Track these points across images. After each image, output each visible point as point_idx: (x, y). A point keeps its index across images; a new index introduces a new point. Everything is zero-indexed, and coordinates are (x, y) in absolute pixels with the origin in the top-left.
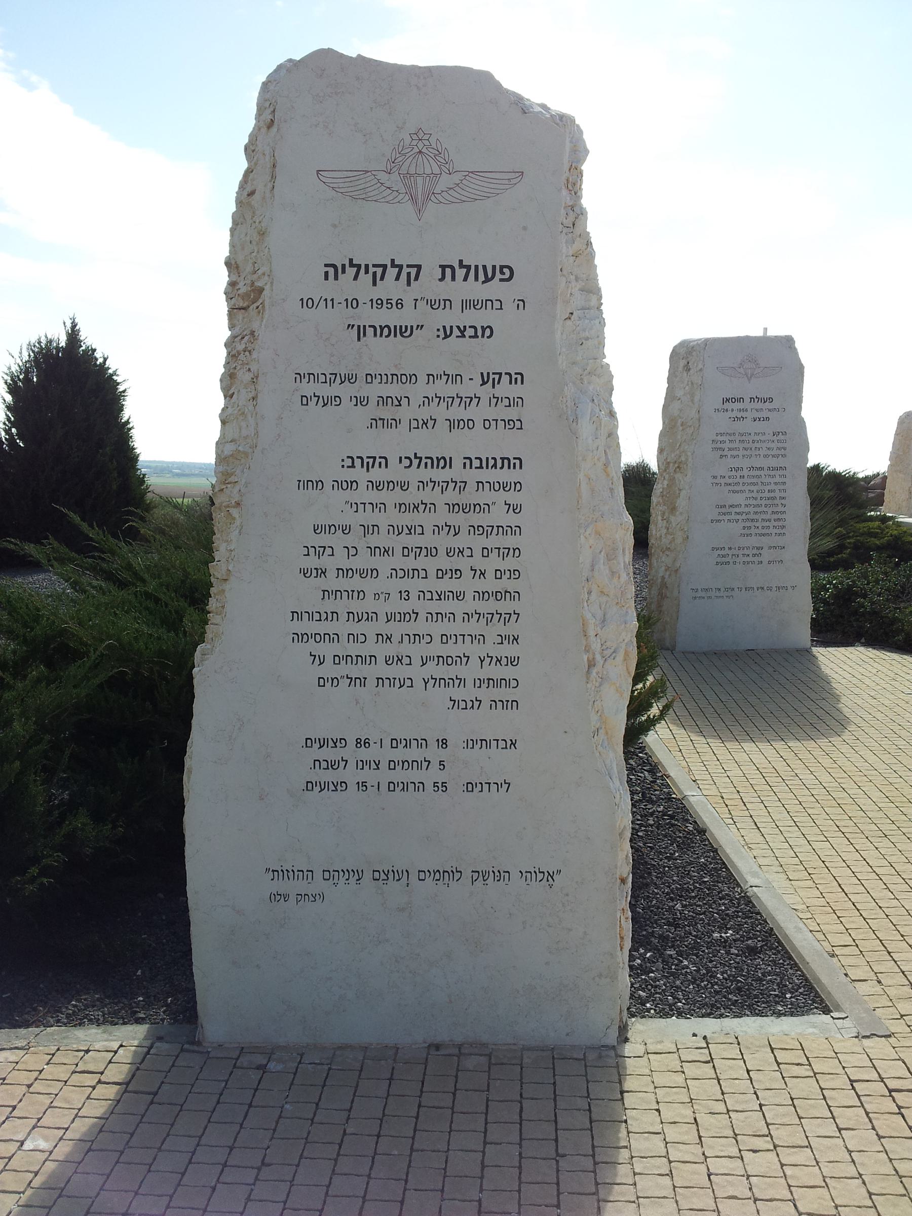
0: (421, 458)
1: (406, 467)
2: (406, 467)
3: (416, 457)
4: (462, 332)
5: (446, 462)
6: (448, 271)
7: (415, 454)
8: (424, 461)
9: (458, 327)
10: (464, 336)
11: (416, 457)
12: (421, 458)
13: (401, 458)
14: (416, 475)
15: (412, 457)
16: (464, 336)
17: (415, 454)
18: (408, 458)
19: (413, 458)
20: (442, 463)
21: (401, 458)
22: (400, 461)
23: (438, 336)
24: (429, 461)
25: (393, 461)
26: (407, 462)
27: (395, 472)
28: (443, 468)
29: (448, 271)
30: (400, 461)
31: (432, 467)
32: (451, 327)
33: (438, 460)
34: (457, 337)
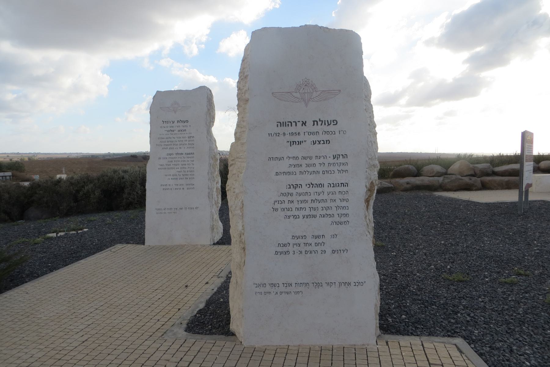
0: (313, 184)
1: (308, 188)
2: (308, 188)
3: (311, 184)
4: (319, 142)
5: (321, 185)
6: (315, 123)
7: (311, 183)
8: (314, 185)
9: (318, 141)
10: (320, 143)
11: (311, 184)
12: (313, 184)
13: (306, 185)
14: (312, 190)
15: (310, 184)
16: (320, 143)
17: (311, 183)
18: (309, 184)
19: (310, 184)
20: (320, 185)
21: (306, 185)
22: (306, 186)
23: (311, 144)
24: (316, 185)
25: (304, 186)
26: (308, 186)
27: (305, 189)
28: (321, 187)
29: (315, 123)
30: (306, 186)
31: (317, 187)
32: (316, 141)
33: (319, 185)
34: (318, 144)
